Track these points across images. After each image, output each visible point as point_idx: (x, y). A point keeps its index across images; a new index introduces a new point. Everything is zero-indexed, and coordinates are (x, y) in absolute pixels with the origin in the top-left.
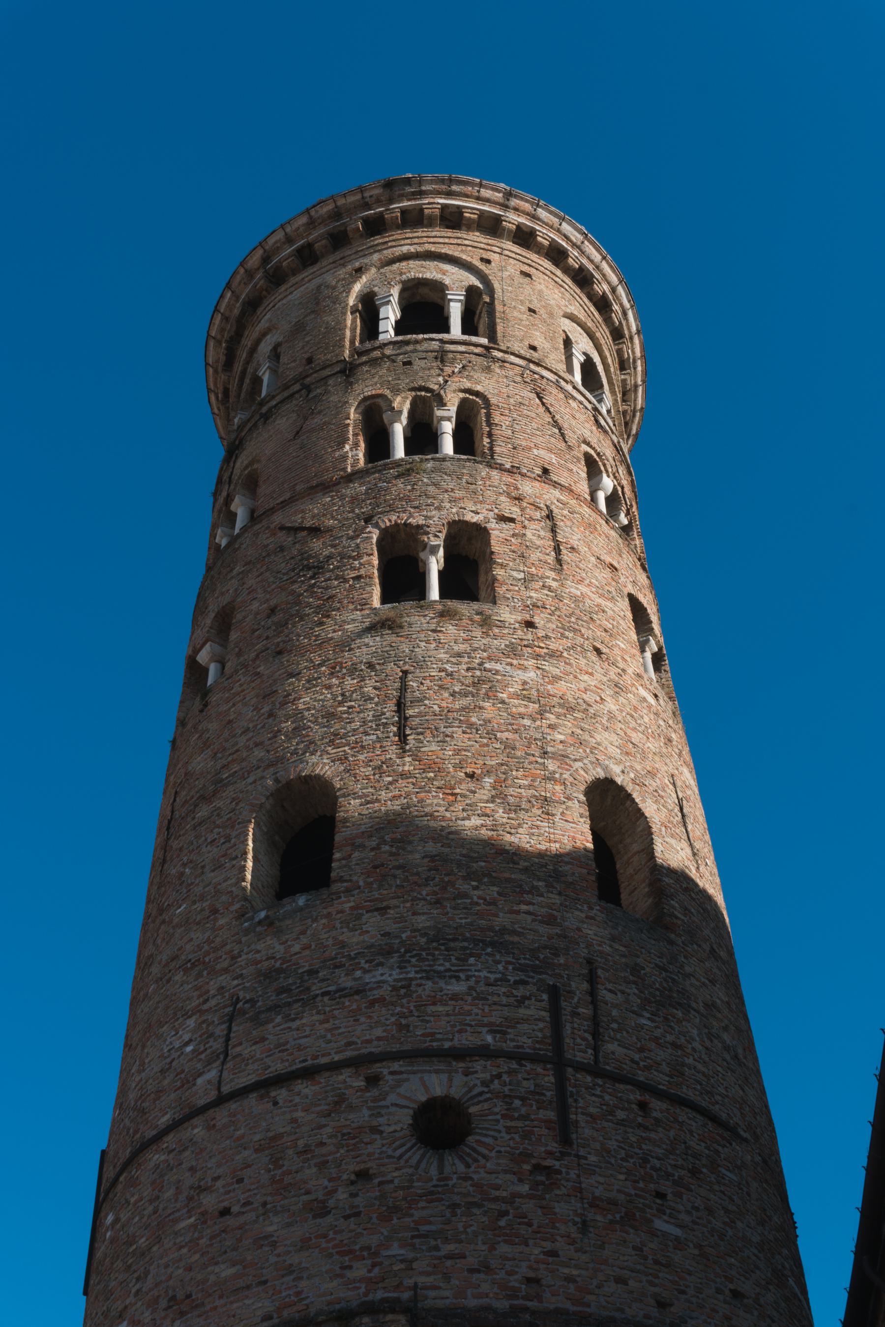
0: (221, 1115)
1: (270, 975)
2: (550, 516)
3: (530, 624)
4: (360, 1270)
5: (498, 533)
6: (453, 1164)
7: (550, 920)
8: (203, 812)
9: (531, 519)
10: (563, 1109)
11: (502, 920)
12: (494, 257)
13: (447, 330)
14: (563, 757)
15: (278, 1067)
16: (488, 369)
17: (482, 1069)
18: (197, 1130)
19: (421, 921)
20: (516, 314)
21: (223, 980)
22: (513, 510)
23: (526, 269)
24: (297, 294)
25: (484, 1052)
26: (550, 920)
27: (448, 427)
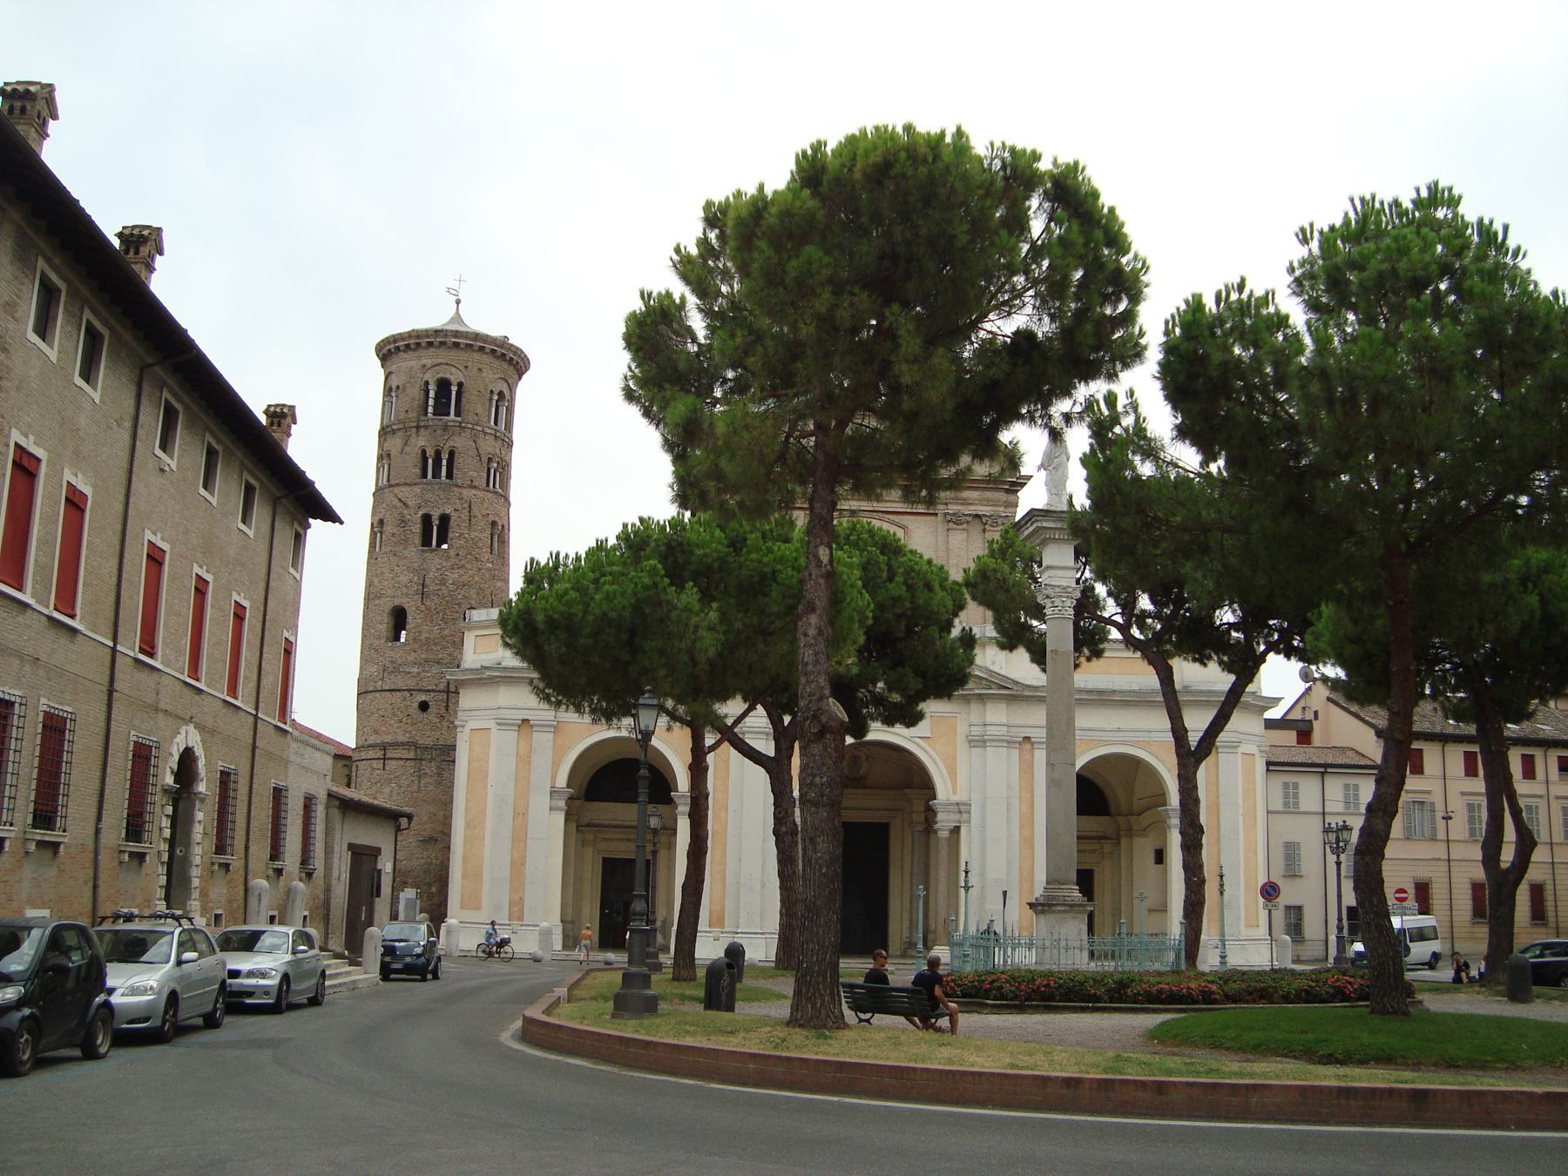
0: (383, 693)
1: (392, 662)
2: (470, 506)
3: (458, 555)
4: (407, 735)
5: (454, 516)
6: (425, 715)
7: (450, 655)
8: (377, 602)
9: (464, 508)
10: (447, 703)
11: (440, 656)
12: (470, 364)
13: (448, 414)
14: (459, 604)
15: (393, 687)
16: (460, 434)
17: (432, 694)
18: (377, 695)
19: (423, 656)
20: (473, 397)
21: (381, 659)
22: (459, 507)
23: (480, 366)
24: (404, 364)
25: (433, 691)
26: (450, 655)
27: (444, 462)
